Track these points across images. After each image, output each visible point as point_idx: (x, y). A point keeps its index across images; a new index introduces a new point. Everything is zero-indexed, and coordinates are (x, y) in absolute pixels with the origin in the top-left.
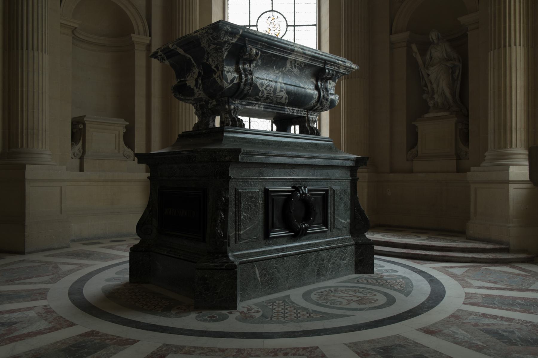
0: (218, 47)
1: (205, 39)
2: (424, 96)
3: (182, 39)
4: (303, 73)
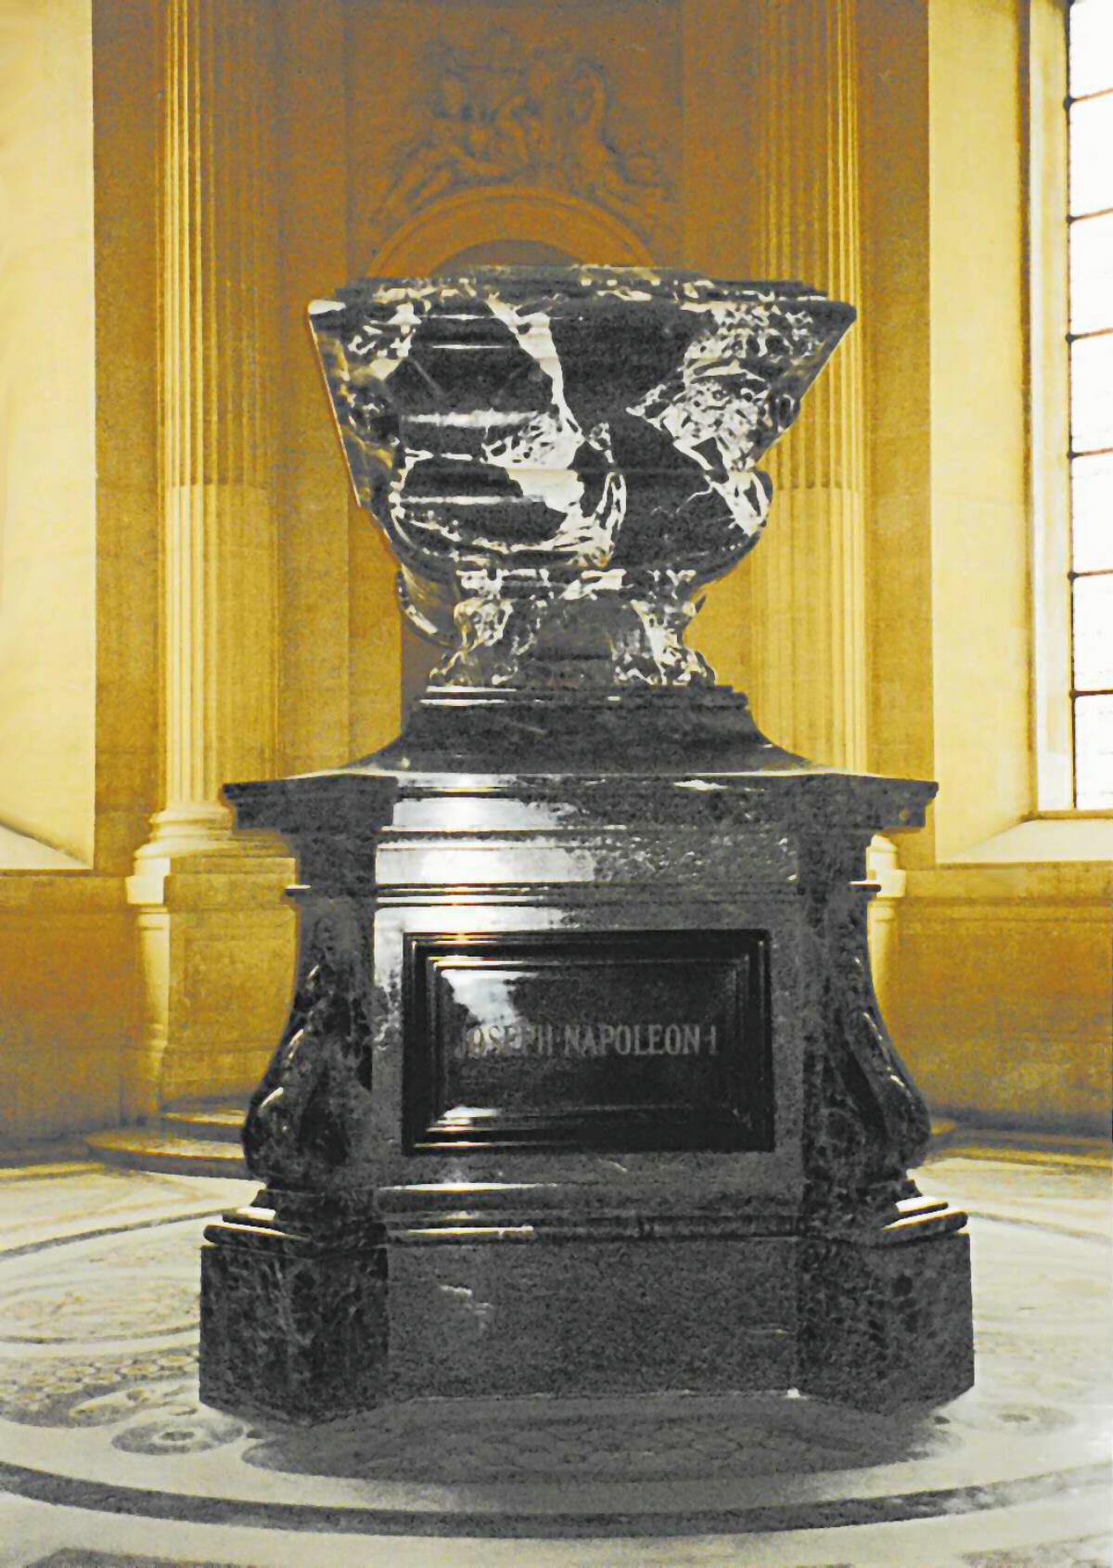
0: (751, 376)
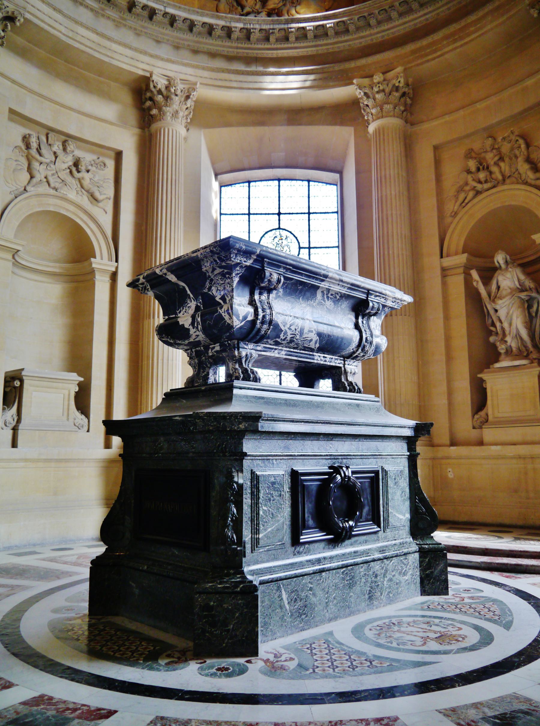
0: (226, 271)
1: (208, 261)
2: (492, 339)
3: (175, 262)
4: (338, 307)
